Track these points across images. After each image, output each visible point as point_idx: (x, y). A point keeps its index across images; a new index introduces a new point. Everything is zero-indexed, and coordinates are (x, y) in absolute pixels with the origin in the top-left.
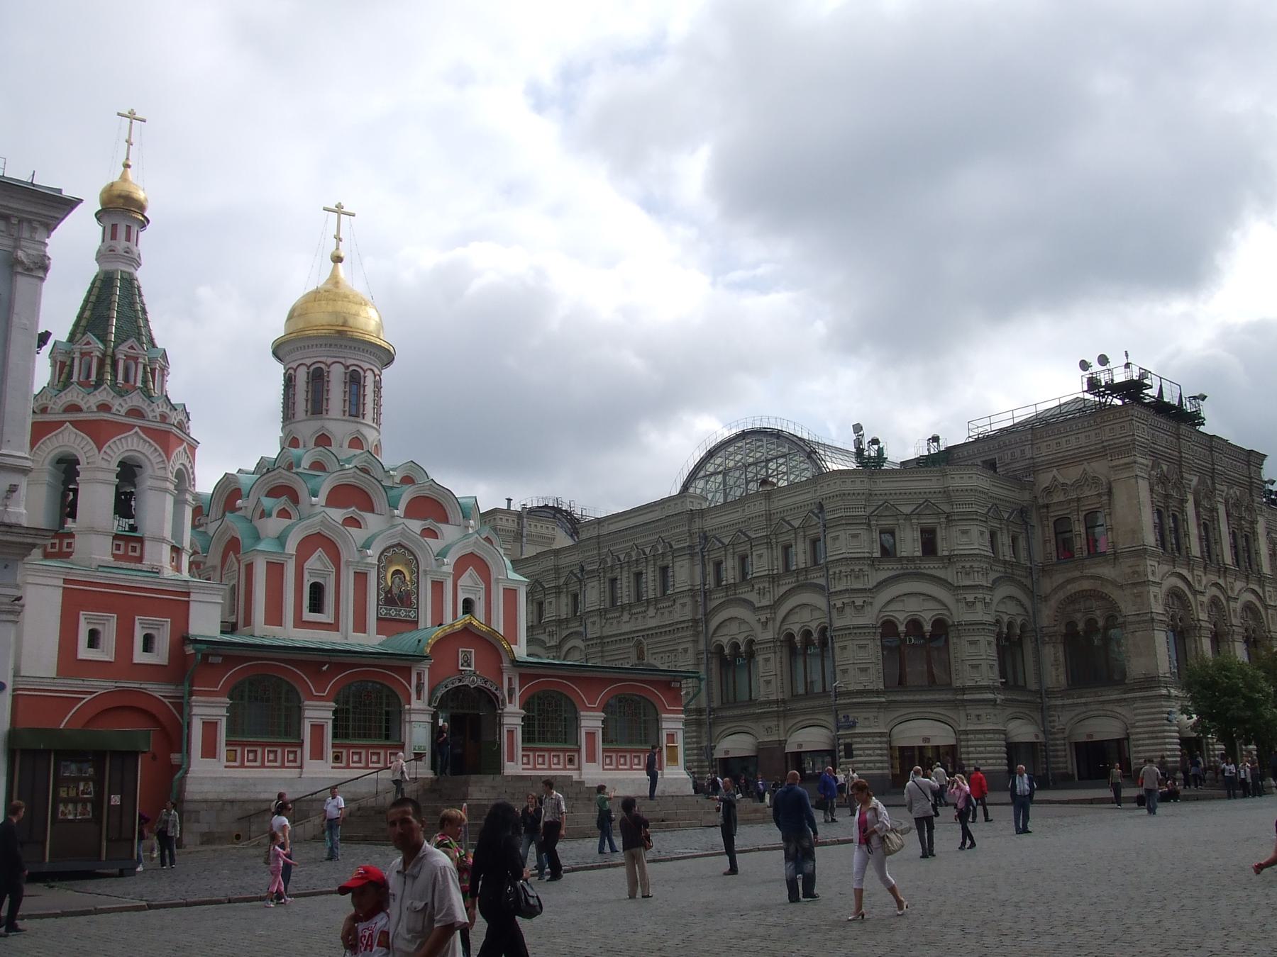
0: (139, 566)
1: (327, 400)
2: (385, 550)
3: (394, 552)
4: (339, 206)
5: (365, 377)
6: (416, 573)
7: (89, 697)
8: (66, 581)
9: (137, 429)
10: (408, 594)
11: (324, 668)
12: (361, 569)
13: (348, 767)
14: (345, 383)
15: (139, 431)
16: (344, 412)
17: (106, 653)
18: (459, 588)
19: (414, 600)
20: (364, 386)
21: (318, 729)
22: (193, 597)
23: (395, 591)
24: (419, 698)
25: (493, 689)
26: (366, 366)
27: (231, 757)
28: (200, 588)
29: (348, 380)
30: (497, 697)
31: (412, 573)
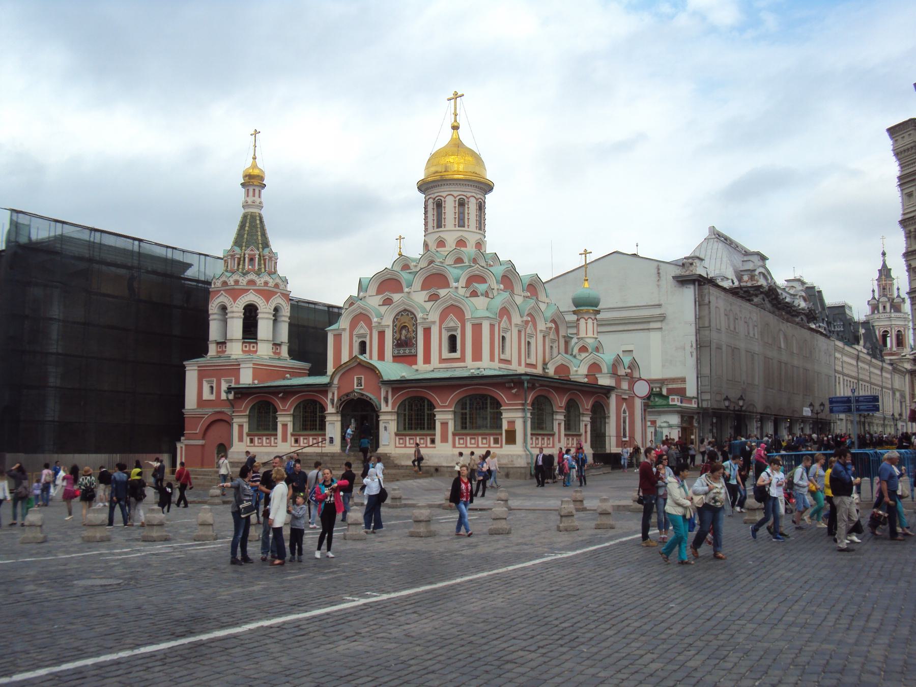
0: (223, 355)
1: (445, 218)
2: (397, 315)
3: (402, 315)
4: (456, 94)
5: (445, 201)
6: (416, 325)
7: (206, 416)
8: (199, 367)
9: (222, 292)
10: (410, 339)
11: (281, 395)
12: (381, 329)
13: (299, 446)
14: (433, 209)
15: (224, 293)
16: (434, 227)
17: (213, 397)
18: (443, 331)
19: (413, 341)
20: (445, 207)
21: (285, 426)
22: (241, 366)
23: (403, 338)
24: (333, 407)
25: (368, 399)
26: (444, 194)
27: (252, 441)
28: (242, 361)
29: (435, 207)
30: (372, 405)
31: (414, 325)
